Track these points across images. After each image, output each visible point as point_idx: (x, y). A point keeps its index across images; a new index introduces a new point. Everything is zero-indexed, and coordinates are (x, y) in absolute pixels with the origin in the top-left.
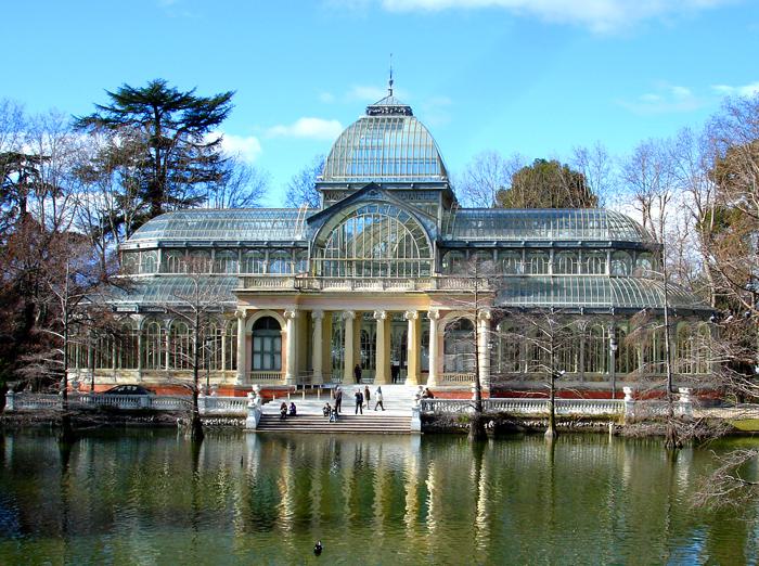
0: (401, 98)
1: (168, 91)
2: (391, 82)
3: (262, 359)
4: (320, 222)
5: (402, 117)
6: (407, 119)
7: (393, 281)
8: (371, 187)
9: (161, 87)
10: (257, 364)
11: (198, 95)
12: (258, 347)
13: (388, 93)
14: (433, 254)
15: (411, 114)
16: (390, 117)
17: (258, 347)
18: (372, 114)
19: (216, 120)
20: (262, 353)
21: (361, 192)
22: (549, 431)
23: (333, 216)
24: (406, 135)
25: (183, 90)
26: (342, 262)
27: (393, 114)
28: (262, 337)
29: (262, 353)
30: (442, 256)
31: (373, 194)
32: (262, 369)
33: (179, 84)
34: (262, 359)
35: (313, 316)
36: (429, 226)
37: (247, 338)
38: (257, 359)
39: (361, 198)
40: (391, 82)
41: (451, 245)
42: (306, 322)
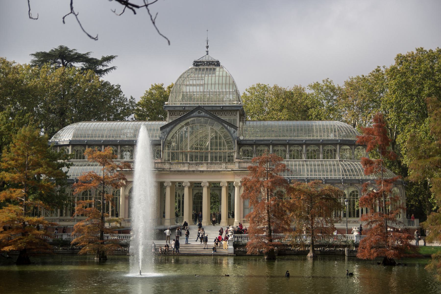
0: (214, 56)
1: (70, 51)
2: (207, 47)
4: (168, 129)
5: (214, 67)
6: (218, 69)
7: (211, 163)
8: (199, 108)
9: (67, 48)
11: (90, 56)
13: (205, 53)
14: (236, 148)
15: (219, 65)
16: (207, 67)
18: (197, 65)
19: (101, 72)
21: (192, 112)
22: (310, 255)
23: (175, 126)
24: (217, 78)
25: (81, 51)
26: (178, 152)
27: (209, 65)
30: (239, 148)
31: (199, 113)
35: (165, 184)
36: (232, 132)
39: (192, 115)
40: (207, 47)
41: (244, 142)
42: (161, 187)
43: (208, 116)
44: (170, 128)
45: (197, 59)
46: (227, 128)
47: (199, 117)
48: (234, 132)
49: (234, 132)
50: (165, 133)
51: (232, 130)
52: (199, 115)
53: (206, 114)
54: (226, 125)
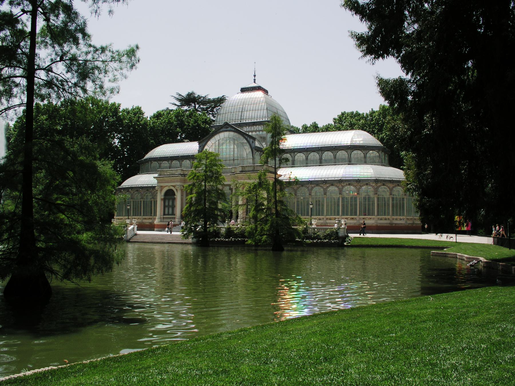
2: (255, 76)
3: (169, 210)
10: (166, 212)
12: (167, 204)
17: (167, 204)
20: (169, 206)
28: (169, 200)
29: (169, 206)
31: (227, 128)
32: (168, 215)
33: (200, 92)
34: (169, 210)
36: (251, 143)
37: (162, 199)
38: (167, 209)
39: (221, 130)
40: (255, 76)
43: (233, 130)
44: (205, 142)
45: (243, 86)
46: (247, 139)
47: (226, 131)
48: (253, 142)
49: (253, 142)
50: (202, 146)
51: (251, 140)
52: (227, 129)
53: (231, 129)
54: (246, 137)
